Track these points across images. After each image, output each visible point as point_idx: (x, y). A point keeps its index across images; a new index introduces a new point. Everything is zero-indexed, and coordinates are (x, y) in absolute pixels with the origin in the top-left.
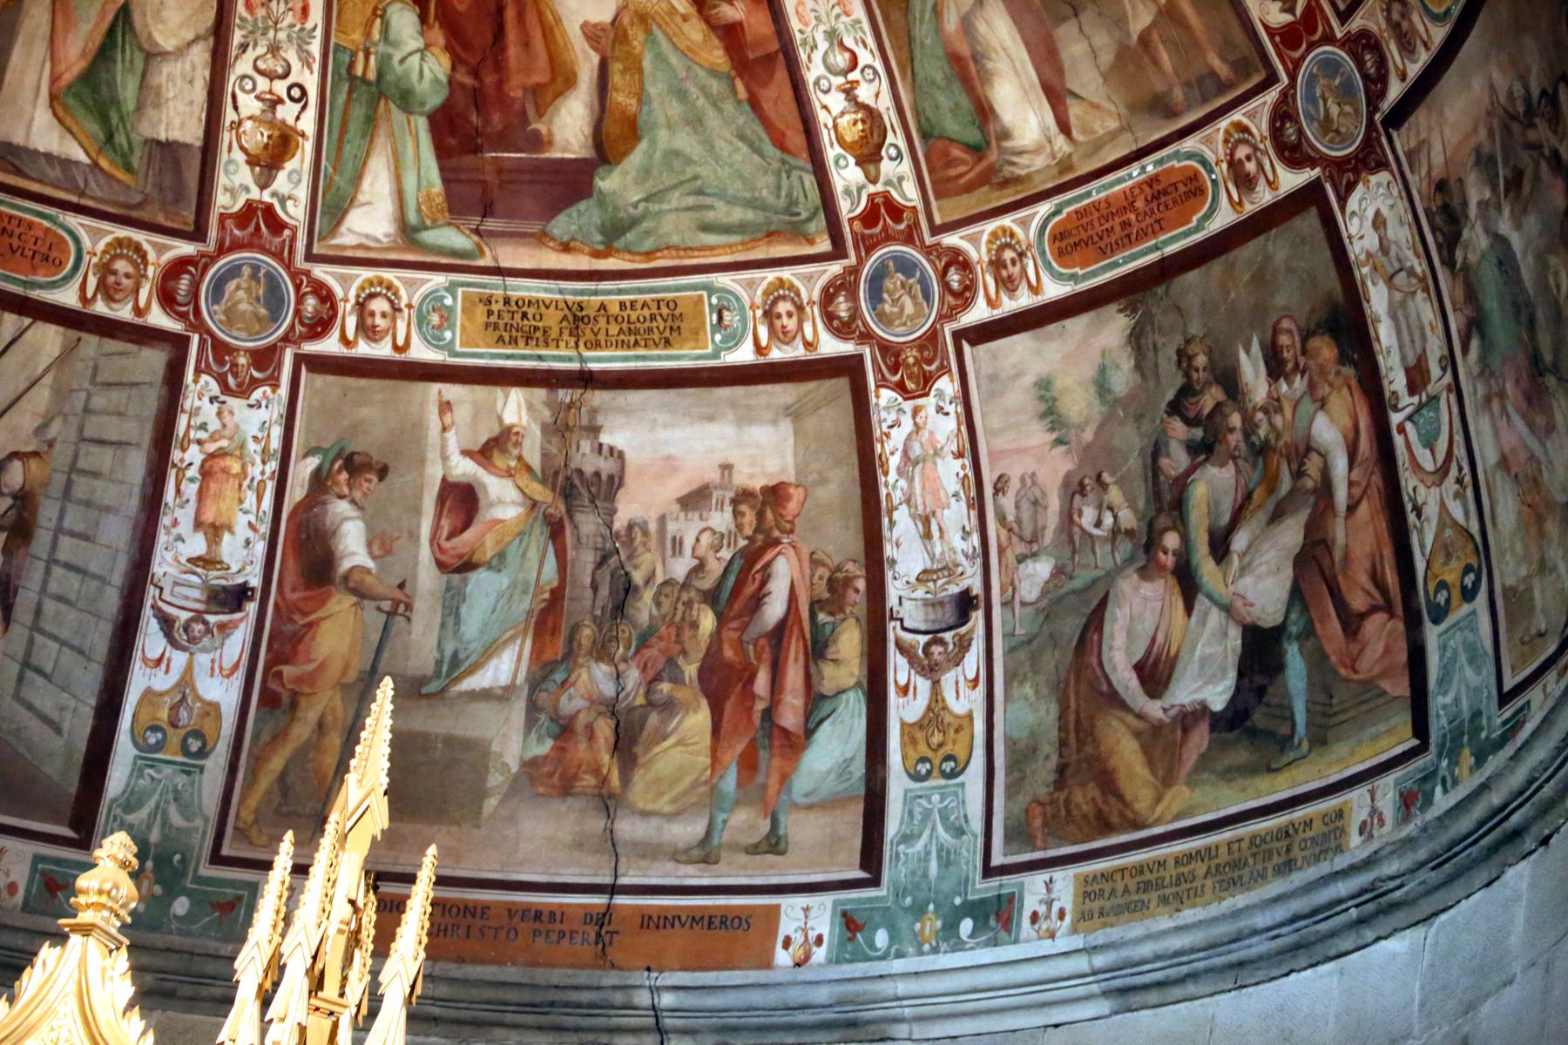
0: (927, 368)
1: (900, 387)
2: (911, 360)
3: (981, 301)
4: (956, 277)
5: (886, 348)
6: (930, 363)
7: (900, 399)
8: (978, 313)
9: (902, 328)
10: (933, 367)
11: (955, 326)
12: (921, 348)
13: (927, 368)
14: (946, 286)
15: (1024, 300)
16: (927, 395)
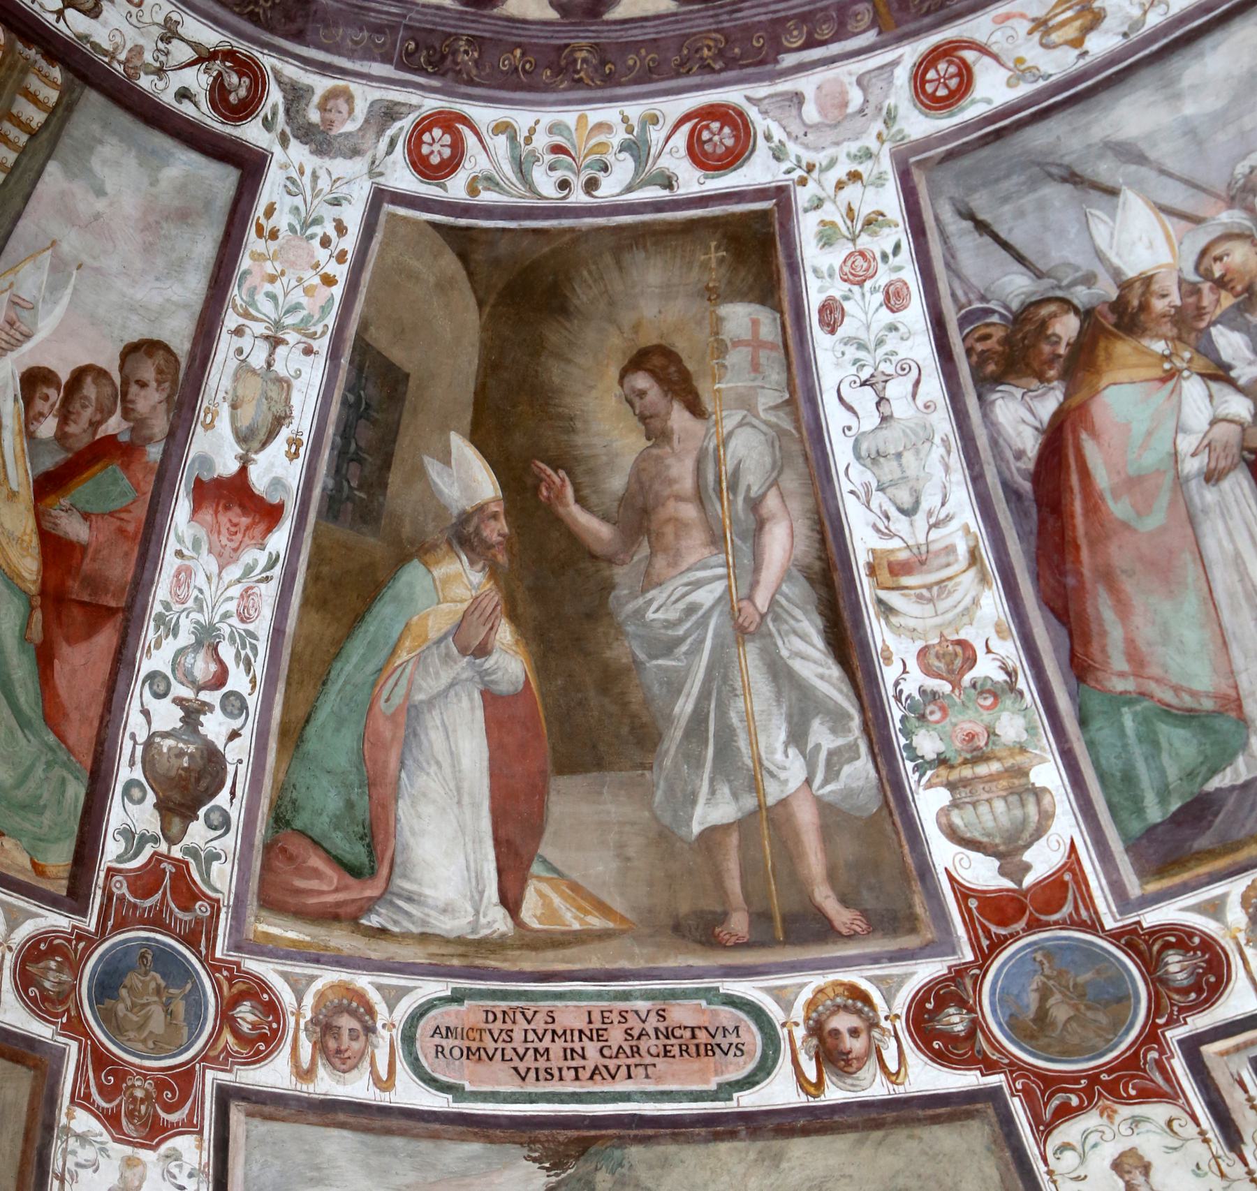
0: (163, 1115)
1: (111, 1120)
2: (139, 1094)
3: (282, 1060)
4: (251, 1018)
5: (101, 1060)
6: (170, 1109)
7: (106, 1137)
8: (273, 1075)
9: (140, 1046)
10: (174, 1117)
11: (225, 1077)
12: (161, 1085)
13: (163, 1115)
14: (226, 1018)
15: (357, 1088)
16: (154, 1148)
